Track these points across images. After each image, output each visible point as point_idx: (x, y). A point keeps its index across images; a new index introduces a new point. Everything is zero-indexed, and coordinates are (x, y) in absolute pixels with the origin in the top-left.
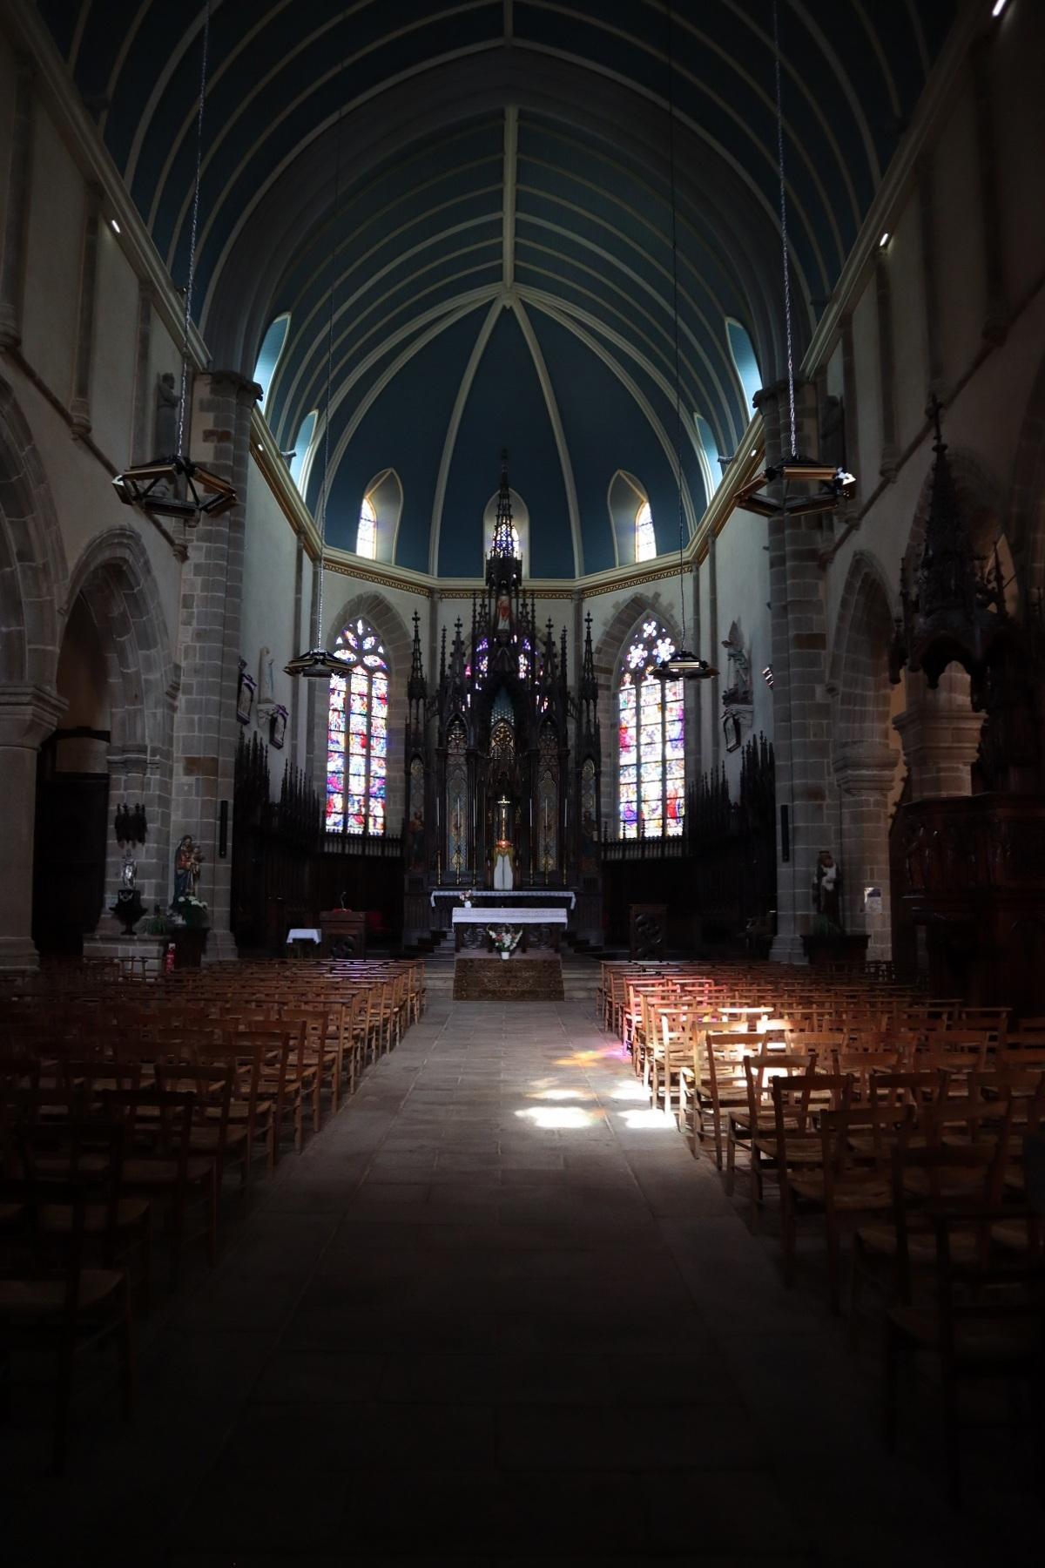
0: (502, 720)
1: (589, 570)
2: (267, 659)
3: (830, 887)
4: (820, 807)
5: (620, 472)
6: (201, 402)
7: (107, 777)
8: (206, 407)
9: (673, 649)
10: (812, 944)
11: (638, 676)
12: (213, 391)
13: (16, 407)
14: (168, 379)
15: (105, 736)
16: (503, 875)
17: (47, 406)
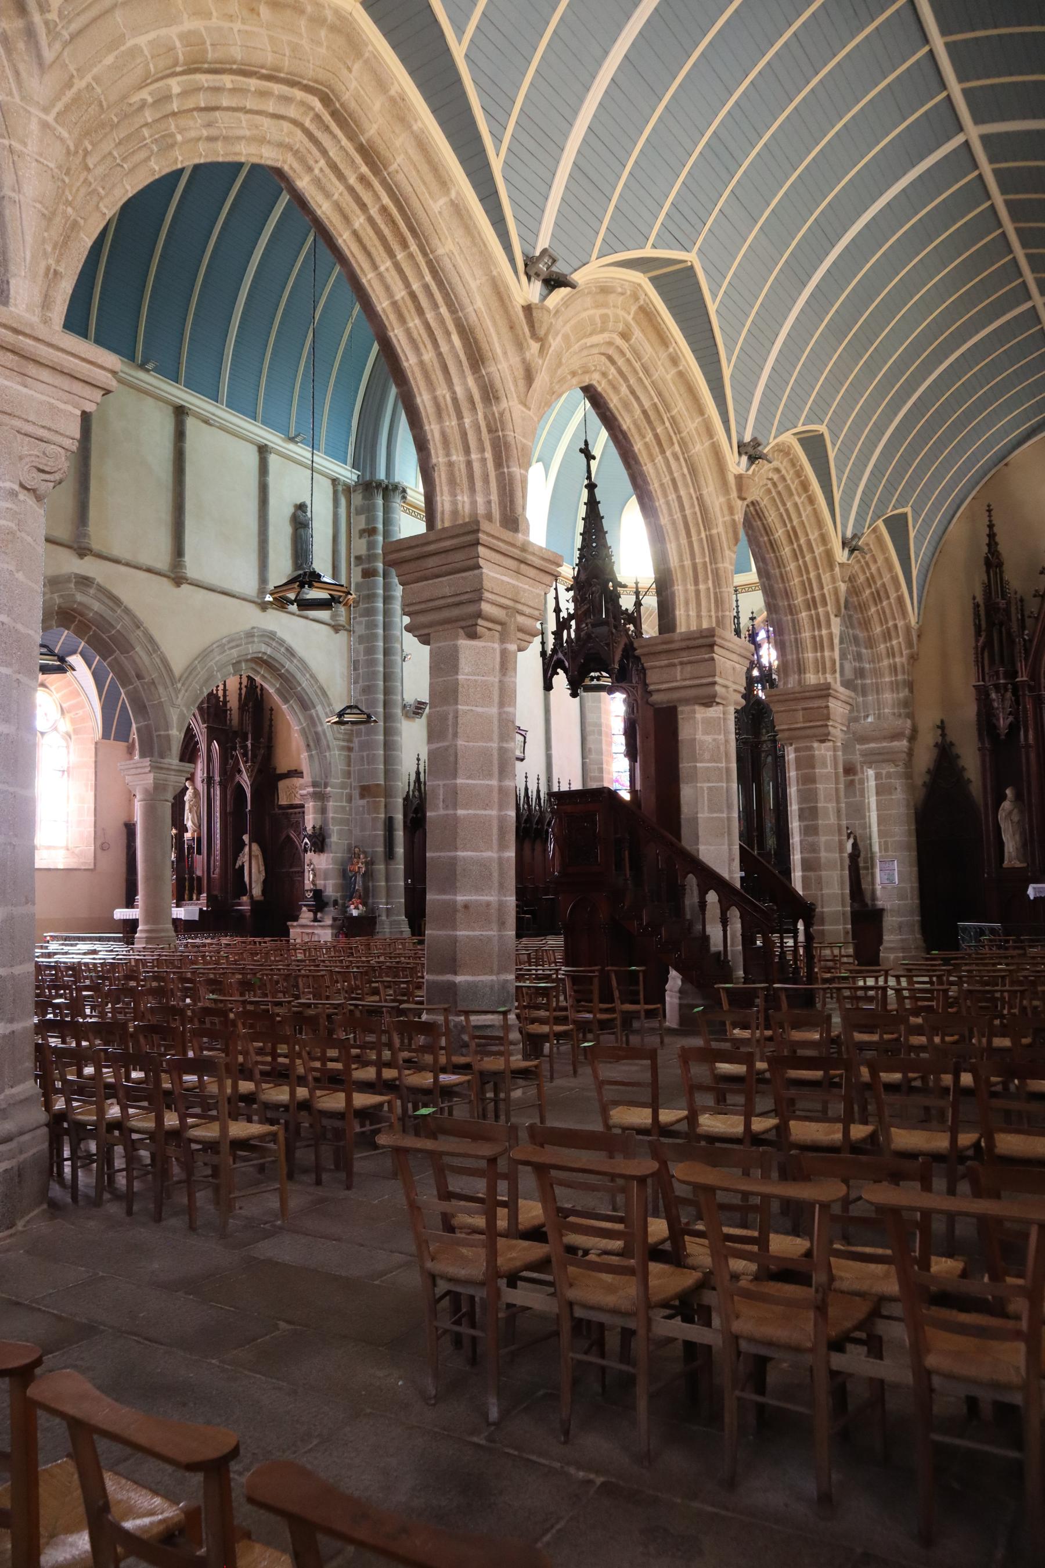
6: (356, 509)
7: (302, 806)
8: (358, 513)
12: (364, 498)
13: (101, 589)
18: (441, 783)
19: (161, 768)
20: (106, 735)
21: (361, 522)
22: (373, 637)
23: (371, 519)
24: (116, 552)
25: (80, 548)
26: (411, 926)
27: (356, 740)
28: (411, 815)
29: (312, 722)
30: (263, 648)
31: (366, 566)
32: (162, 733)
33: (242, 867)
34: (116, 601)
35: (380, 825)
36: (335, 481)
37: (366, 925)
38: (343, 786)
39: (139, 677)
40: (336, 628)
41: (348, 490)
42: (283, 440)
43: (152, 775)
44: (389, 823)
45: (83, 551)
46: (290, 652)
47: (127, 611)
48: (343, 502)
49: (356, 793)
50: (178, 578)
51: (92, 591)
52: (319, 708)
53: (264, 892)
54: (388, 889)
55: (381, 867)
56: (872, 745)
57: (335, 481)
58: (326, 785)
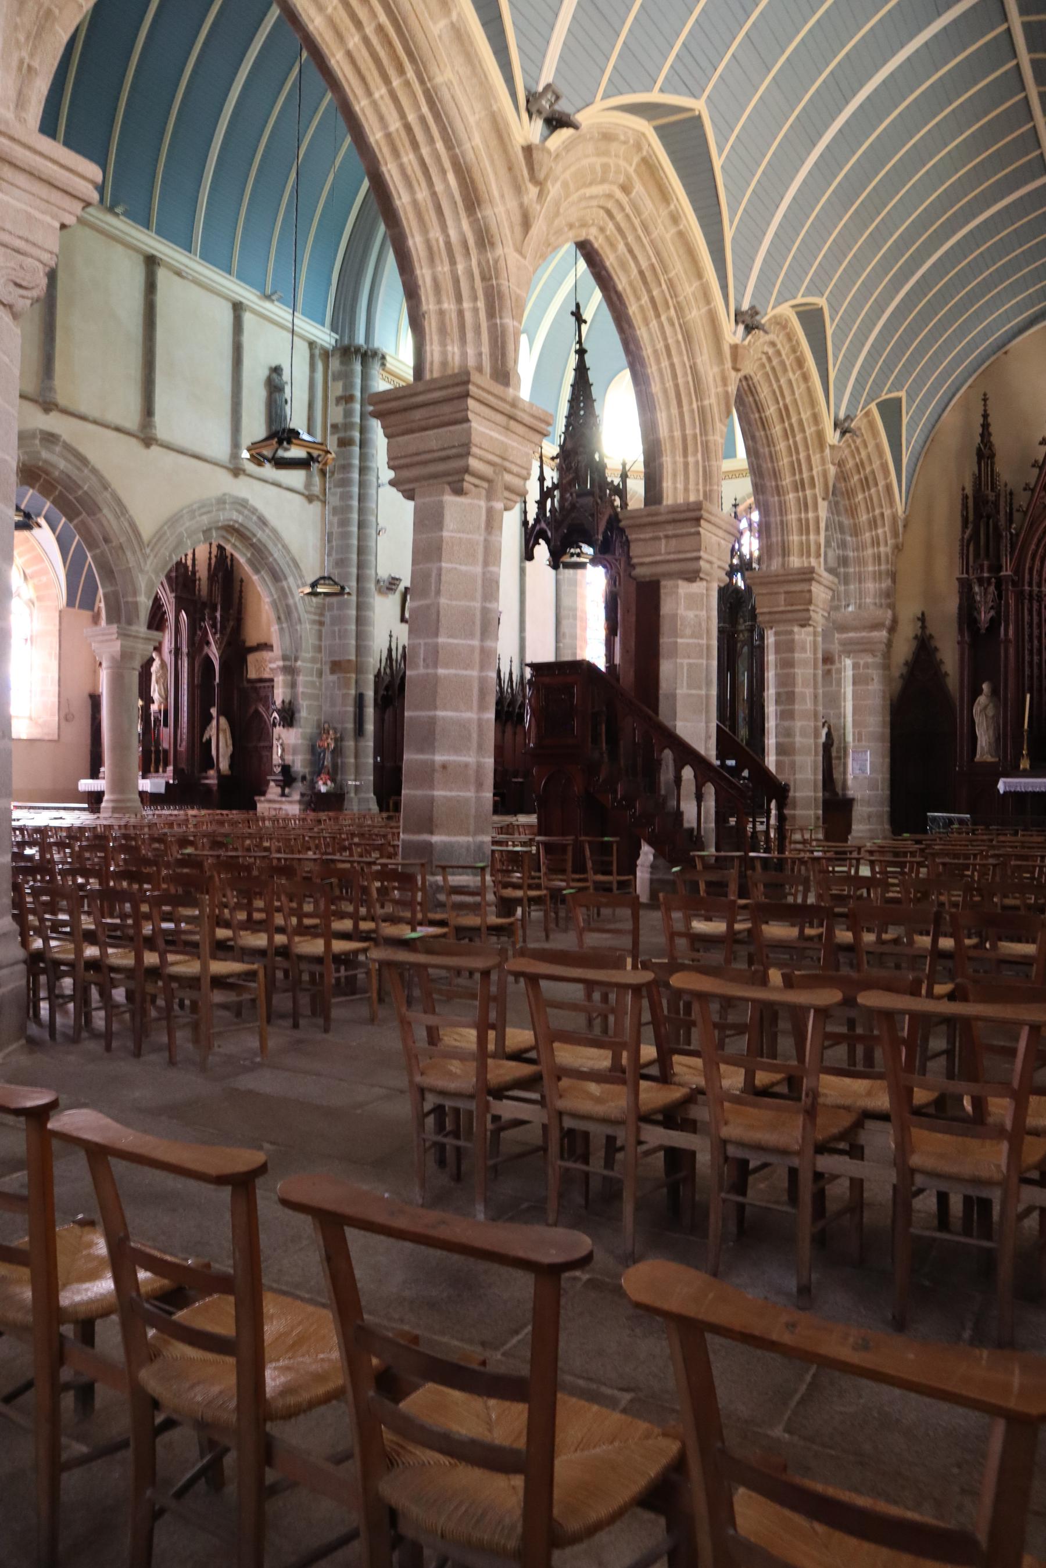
7: (272, 680)
8: (335, 379)
12: (342, 363)
13: (67, 447)
17: (115, 434)
18: (422, 641)
19: (129, 636)
20: (70, 603)
21: (337, 389)
22: (348, 509)
23: (349, 385)
24: (83, 409)
25: (45, 402)
26: (380, 803)
27: (328, 614)
28: (382, 692)
29: (284, 594)
30: (235, 516)
31: (342, 435)
33: (209, 741)
34: (84, 461)
35: (351, 701)
36: (312, 344)
37: (335, 801)
38: (313, 660)
39: (106, 540)
40: (310, 499)
41: (326, 355)
42: (260, 298)
43: (118, 643)
44: (360, 699)
45: (48, 406)
46: (263, 522)
47: (94, 471)
48: (320, 366)
49: (327, 669)
50: (147, 438)
51: (58, 449)
52: (291, 580)
53: (231, 766)
54: (357, 767)
55: (350, 744)
56: (852, 635)
57: (312, 344)
58: (296, 660)
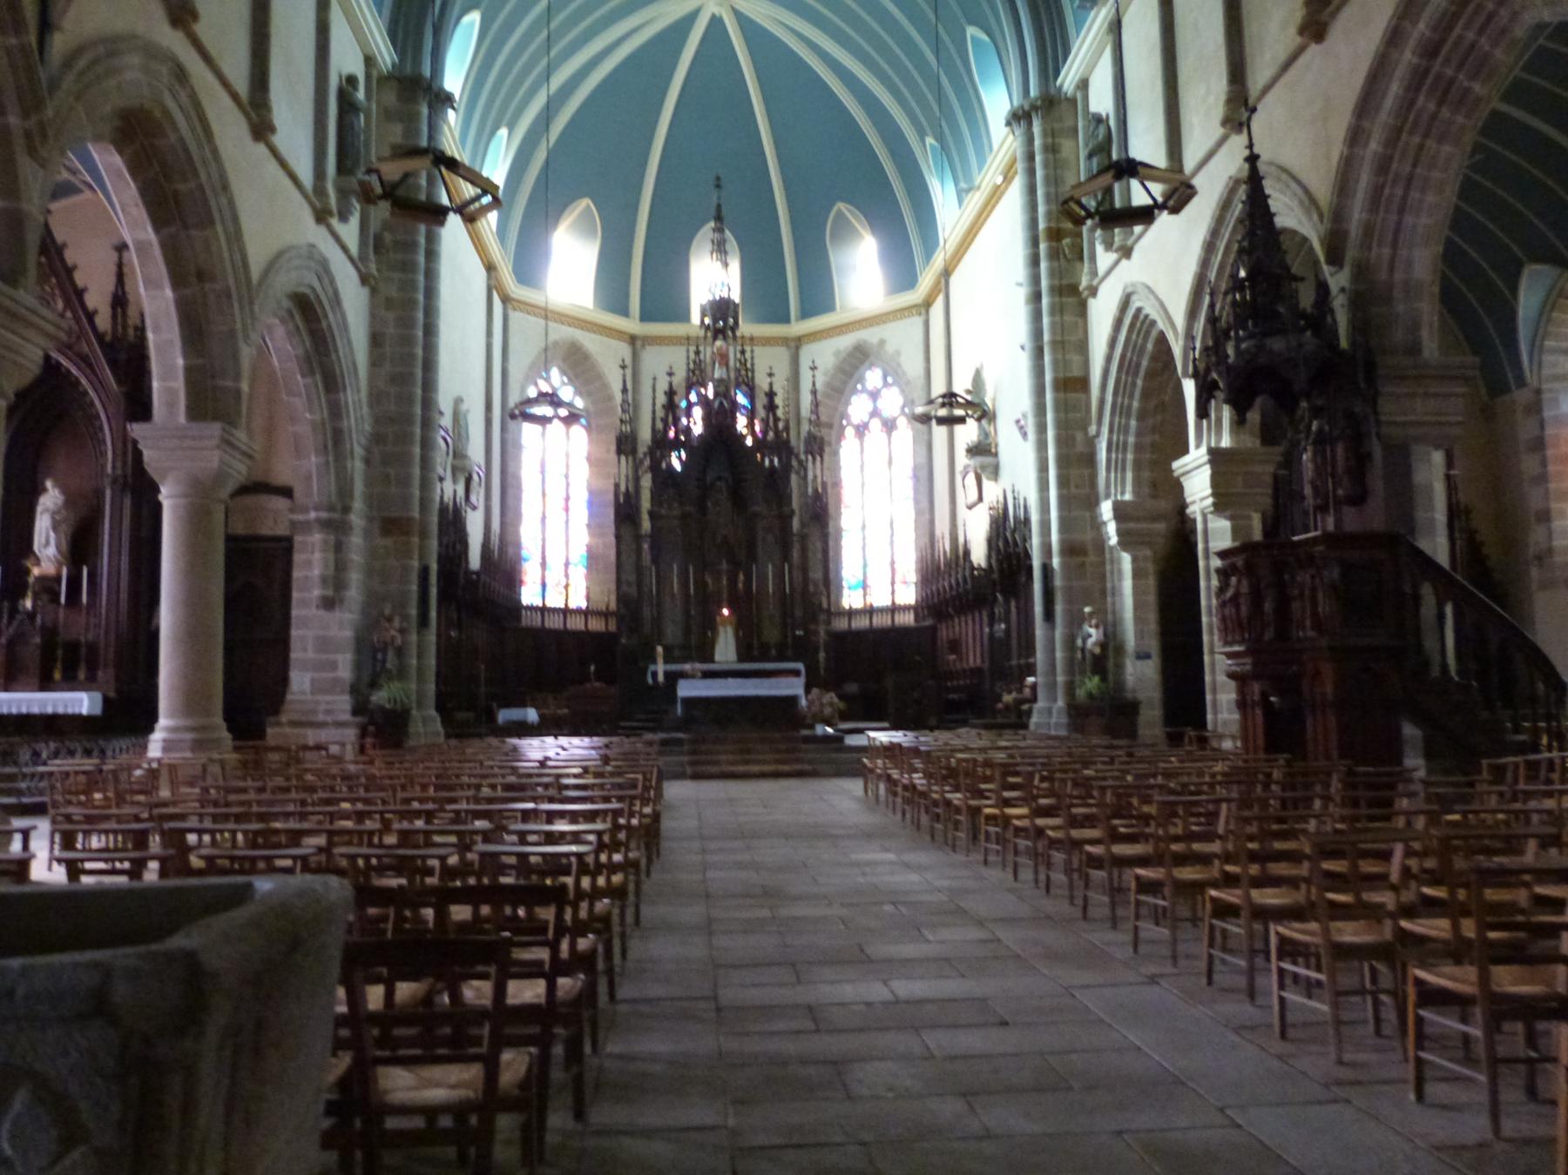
0: (720, 478)
1: (805, 314)
2: (464, 407)
3: (1097, 650)
4: (1083, 565)
5: (841, 206)
9: (900, 401)
10: (1078, 713)
11: (861, 430)
14: (352, 80)
15: (287, 492)
16: (725, 649)
29: (336, 411)
32: (229, 383)
44: (424, 573)
52: (349, 391)
